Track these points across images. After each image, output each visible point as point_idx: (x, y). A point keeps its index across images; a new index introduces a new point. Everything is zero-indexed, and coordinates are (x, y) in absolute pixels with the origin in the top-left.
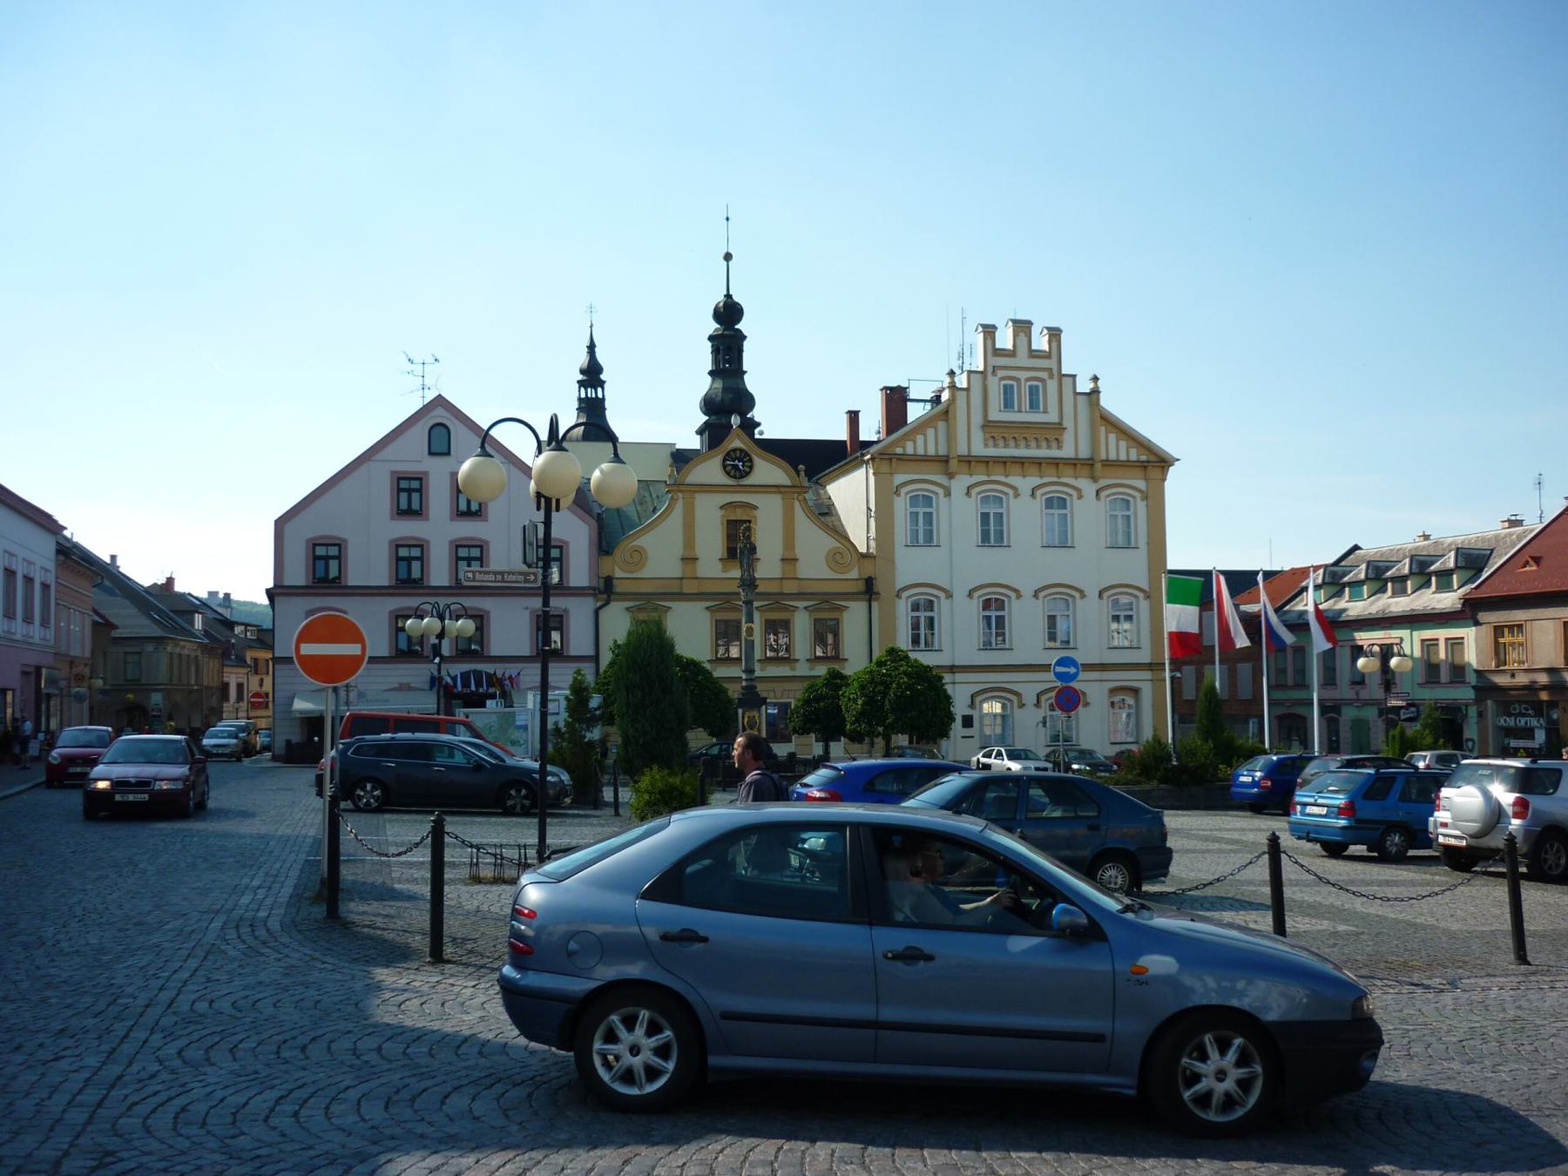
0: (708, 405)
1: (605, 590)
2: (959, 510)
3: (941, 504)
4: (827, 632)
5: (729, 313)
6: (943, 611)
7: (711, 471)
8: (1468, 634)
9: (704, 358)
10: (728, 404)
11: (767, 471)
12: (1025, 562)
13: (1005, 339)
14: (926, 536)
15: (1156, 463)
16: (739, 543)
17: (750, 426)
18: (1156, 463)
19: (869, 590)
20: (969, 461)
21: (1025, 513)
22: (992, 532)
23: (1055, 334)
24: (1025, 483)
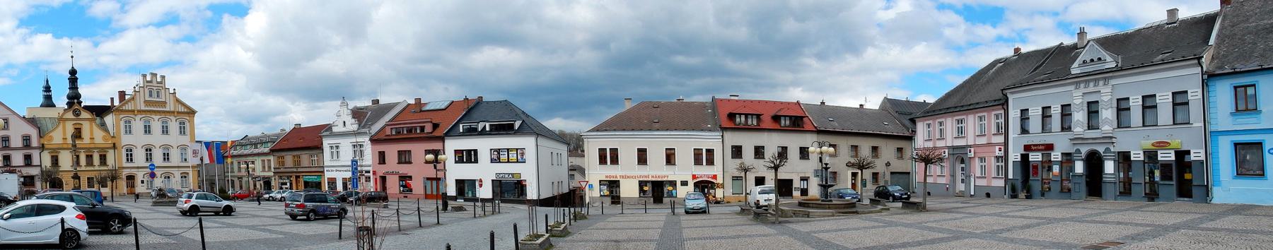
0: (69, 97)
1: (42, 148)
2: (138, 125)
3: (133, 124)
4: (103, 159)
5: (73, 72)
6: (135, 152)
7: (70, 115)
8: (271, 158)
9: (67, 84)
10: (74, 98)
11: (85, 115)
12: (157, 139)
13: (149, 78)
14: (129, 131)
15: (192, 113)
16: (78, 134)
17: (80, 103)
18: (192, 113)
19: (114, 147)
20: (140, 111)
21: (156, 126)
22: (147, 130)
23: (163, 77)
24: (156, 117)
